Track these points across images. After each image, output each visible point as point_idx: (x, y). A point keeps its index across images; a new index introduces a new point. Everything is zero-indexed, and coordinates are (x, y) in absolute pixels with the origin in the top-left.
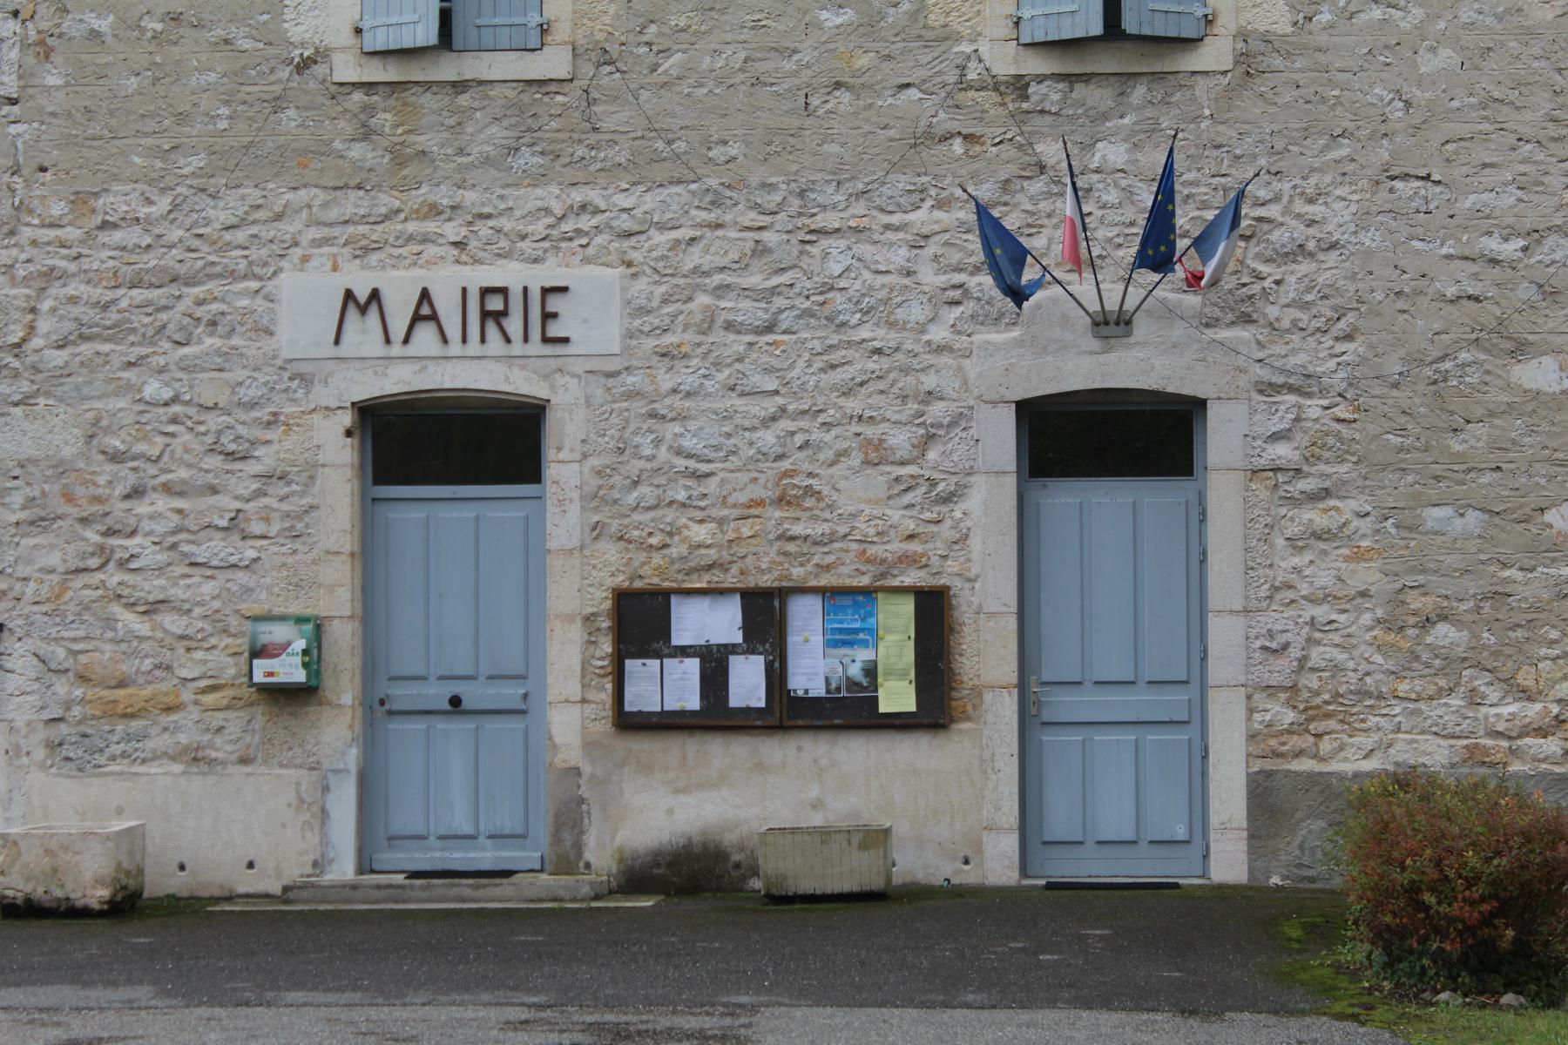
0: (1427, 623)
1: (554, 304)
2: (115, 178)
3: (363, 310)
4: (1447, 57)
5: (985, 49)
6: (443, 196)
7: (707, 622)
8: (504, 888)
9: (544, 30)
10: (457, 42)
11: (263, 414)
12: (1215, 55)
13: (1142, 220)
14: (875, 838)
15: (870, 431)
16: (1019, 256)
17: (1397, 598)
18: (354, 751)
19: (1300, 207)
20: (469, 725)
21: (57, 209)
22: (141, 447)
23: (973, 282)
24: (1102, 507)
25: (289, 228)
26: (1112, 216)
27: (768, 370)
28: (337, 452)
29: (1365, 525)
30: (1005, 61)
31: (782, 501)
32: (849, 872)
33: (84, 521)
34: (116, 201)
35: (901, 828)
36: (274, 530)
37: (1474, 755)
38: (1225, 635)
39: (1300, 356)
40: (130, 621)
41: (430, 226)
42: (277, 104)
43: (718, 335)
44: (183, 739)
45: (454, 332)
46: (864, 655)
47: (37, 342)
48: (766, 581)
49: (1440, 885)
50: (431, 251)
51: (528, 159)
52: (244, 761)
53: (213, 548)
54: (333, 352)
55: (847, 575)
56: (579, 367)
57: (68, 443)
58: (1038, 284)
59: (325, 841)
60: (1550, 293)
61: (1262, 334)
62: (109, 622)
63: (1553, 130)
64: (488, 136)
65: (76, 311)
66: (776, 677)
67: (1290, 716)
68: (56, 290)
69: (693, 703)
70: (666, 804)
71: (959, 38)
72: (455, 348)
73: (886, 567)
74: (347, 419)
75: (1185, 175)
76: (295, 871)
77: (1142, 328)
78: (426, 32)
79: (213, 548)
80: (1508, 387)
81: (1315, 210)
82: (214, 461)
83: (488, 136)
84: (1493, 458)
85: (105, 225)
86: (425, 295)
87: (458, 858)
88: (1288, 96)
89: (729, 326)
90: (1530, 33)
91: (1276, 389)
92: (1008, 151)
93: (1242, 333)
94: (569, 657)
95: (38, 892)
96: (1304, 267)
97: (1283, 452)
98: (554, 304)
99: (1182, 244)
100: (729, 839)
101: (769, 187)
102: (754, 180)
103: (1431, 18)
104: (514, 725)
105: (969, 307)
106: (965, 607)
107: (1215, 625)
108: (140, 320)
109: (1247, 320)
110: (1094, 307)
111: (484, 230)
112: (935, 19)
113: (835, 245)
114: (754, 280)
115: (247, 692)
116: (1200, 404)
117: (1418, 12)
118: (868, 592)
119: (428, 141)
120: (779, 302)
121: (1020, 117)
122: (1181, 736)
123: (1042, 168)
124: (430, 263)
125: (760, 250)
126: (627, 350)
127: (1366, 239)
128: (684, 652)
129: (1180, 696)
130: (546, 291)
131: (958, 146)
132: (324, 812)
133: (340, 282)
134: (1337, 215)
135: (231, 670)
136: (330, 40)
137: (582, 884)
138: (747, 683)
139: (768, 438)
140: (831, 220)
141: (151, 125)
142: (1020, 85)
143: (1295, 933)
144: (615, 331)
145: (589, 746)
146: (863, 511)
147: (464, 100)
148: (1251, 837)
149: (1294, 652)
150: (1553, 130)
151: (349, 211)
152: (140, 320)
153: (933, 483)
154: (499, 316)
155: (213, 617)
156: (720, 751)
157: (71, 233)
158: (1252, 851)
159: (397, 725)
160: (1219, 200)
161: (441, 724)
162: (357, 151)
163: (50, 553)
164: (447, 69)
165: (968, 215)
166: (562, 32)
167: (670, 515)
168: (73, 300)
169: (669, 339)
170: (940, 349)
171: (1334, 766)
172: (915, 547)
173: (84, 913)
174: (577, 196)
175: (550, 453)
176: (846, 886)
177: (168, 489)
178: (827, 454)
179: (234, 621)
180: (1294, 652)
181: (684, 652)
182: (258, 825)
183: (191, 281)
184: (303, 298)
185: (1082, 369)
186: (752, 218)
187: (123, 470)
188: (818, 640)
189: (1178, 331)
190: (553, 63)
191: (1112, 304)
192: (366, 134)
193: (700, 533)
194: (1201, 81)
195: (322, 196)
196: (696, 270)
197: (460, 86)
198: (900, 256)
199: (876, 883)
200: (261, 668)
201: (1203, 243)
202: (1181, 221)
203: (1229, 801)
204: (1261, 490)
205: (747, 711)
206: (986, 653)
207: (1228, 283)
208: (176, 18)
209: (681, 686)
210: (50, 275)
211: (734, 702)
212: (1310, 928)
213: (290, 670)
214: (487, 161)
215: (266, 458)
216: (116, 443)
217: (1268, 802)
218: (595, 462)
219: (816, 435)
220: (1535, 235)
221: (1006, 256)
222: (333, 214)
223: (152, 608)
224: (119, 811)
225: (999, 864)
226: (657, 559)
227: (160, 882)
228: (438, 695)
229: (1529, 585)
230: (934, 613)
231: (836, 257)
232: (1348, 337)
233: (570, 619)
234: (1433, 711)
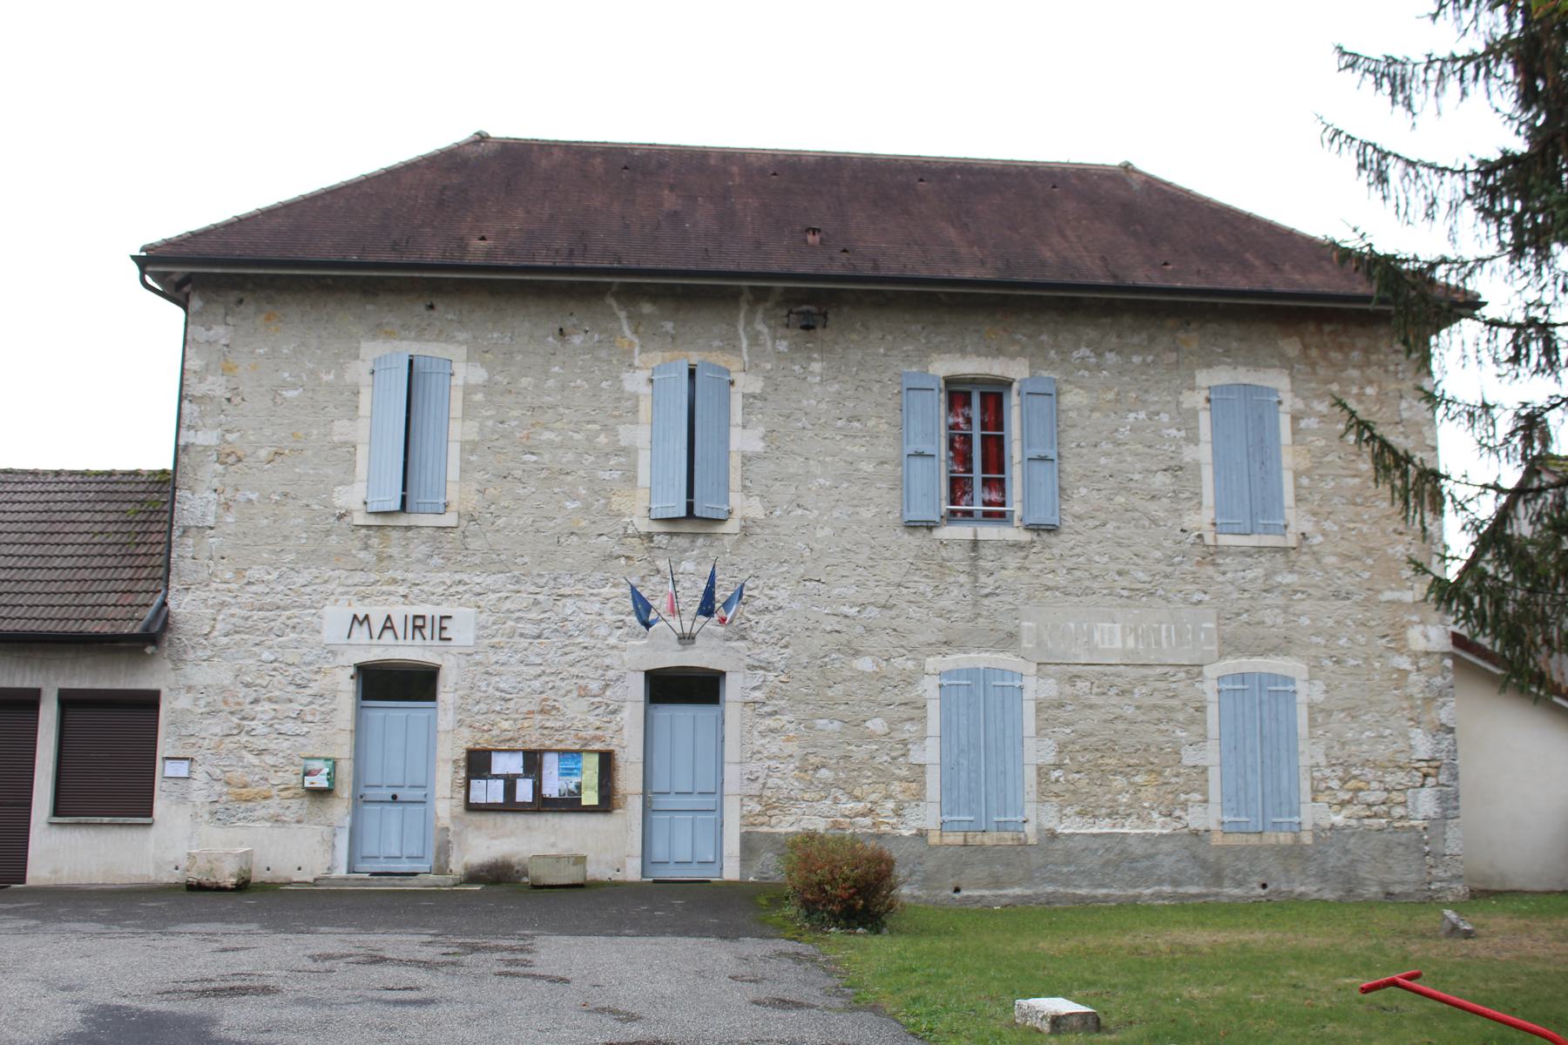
1: (446, 623)
3: (361, 623)
4: (828, 531)
5: (635, 520)
6: (399, 575)
8: (414, 880)
9: (446, 506)
10: (408, 508)
11: (314, 668)
12: (732, 526)
13: (700, 595)
14: (580, 860)
16: (648, 608)
17: (804, 758)
18: (348, 818)
20: (400, 807)
21: (228, 575)
22: (259, 681)
23: (627, 619)
24: (682, 717)
25: (330, 587)
26: (688, 593)
27: (538, 655)
28: (346, 687)
29: (791, 727)
30: (644, 526)
31: (542, 711)
32: (567, 875)
34: (254, 573)
37: (836, 825)
38: (732, 773)
39: (767, 654)
40: (250, 758)
41: (392, 588)
42: (328, 533)
43: (517, 639)
44: (271, 811)
45: (400, 634)
46: (576, 780)
47: (215, 633)
48: (534, 746)
50: (392, 598)
51: (437, 560)
52: (299, 822)
53: (289, 727)
54: (346, 641)
56: (455, 651)
57: (226, 678)
58: (656, 621)
59: (333, 859)
60: (869, 630)
61: (750, 644)
62: (241, 758)
64: (419, 550)
65: (233, 620)
66: (537, 789)
67: (759, 808)
68: (225, 611)
69: (500, 800)
72: (401, 641)
73: (587, 741)
74: (352, 671)
75: (719, 576)
77: (699, 640)
78: (396, 505)
79: (289, 727)
80: (851, 669)
81: (773, 593)
82: (292, 688)
83: (419, 550)
85: (249, 583)
86: (389, 618)
88: (762, 544)
89: (521, 635)
90: (861, 523)
91: (756, 668)
95: (204, 879)
96: (768, 617)
97: (758, 695)
98: (446, 623)
99: (717, 605)
100: (514, 860)
101: (541, 576)
102: (535, 572)
104: (420, 808)
106: (621, 759)
107: (727, 768)
108: (262, 625)
109: (743, 638)
111: (416, 590)
112: (614, 507)
113: (568, 601)
114: (533, 615)
115: (301, 791)
116: (723, 674)
117: (816, 512)
118: (578, 752)
119: (394, 551)
120: (544, 625)
122: (712, 816)
123: (658, 571)
125: (536, 603)
126: (476, 644)
127: (793, 605)
128: (497, 777)
129: (711, 799)
130: (442, 618)
131: (623, 561)
132: (334, 846)
134: (782, 595)
135: (294, 780)
137: (449, 879)
138: (524, 791)
139: (537, 684)
140: (567, 591)
141: (272, 540)
145: (454, 818)
146: (577, 718)
147: (410, 534)
149: (761, 781)
151: (357, 580)
152: (262, 625)
153: (608, 705)
154: (420, 628)
157: (233, 586)
158: (742, 866)
160: (732, 587)
161: (387, 807)
162: (362, 554)
163: (216, 727)
164: (403, 520)
165: (627, 590)
166: (454, 506)
167: (493, 716)
168: (233, 615)
169: (495, 640)
170: (613, 647)
171: (777, 830)
172: (599, 733)
173: (224, 889)
174: (457, 577)
176: (567, 881)
177: (270, 700)
178: (562, 692)
179: (297, 760)
180: (761, 781)
181: (497, 777)
182: (303, 850)
183: (285, 609)
184: (335, 618)
187: (250, 691)
188: (556, 773)
189: (715, 642)
190: (449, 519)
191: (687, 631)
192: (366, 547)
193: (506, 725)
195: (346, 573)
196: (508, 610)
197: (408, 528)
199: (580, 880)
200: (308, 781)
201: (727, 605)
203: (732, 845)
205: (524, 803)
206: (629, 780)
207: (736, 622)
209: (494, 792)
210: (223, 604)
211: (519, 799)
212: (770, 900)
213: (321, 782)
214: (419, 561)
215: (315, 688)
216: (248, 679)
217: (749, 845)
218: (460, 693)
219: (558, 683)
221: (642, 608)
222: (350, 582)
223: (260, 753)
224: (241, 843)
225: (632, 872)
226: (486, 736)
227: (259, 876)
228: (386, 794)
229: (860, 753)
230: (607, 761)
231: (569, 606)
232: (786, 647)
233: (446, 761)
234: (819, 806)
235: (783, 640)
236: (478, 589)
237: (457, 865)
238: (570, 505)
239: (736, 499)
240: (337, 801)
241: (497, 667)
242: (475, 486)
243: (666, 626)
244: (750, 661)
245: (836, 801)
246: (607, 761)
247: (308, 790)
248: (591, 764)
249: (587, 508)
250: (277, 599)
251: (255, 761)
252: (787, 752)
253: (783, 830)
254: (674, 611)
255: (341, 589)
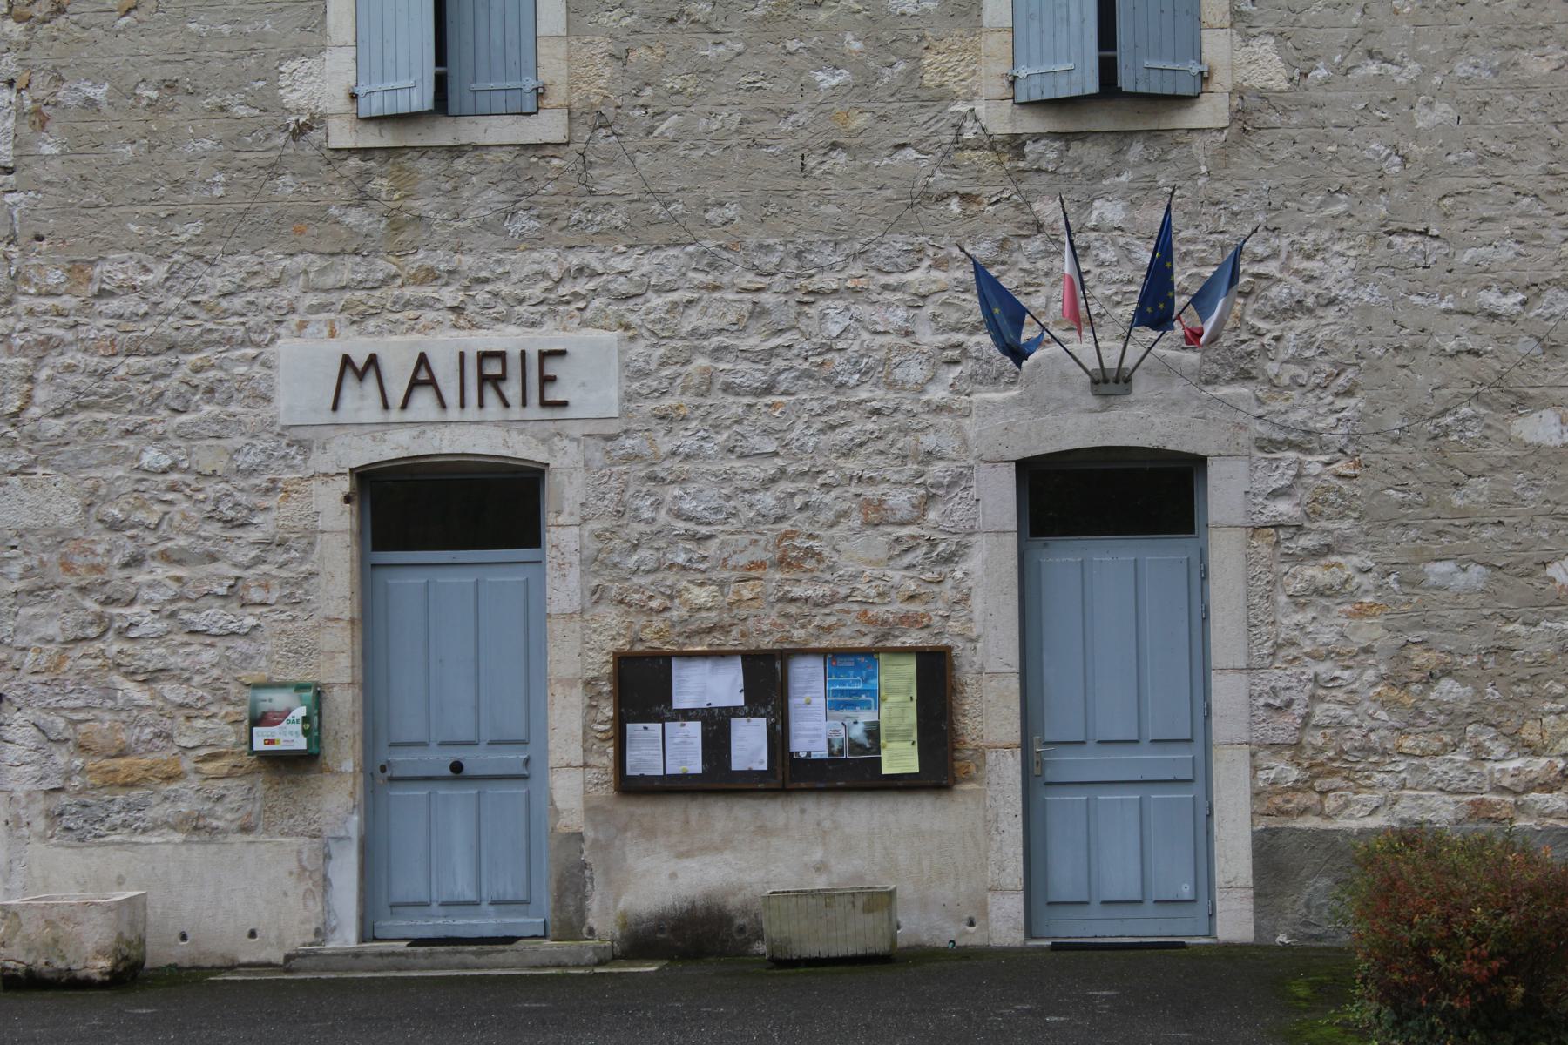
0: (1431, 679)
1: (552, 367)
2: (112, 246)
3: (361, 376)
4: (1443, 111)
5: (980, 109)
7: (710, 685)
8: (508, 955)
9: (539, 94)
10: (453, 106)
11: (261, 480)
12: (1211, 112)
13: (1140, 277)
14: (880, 901)
15: (870, 492)
16: (1018, 315)
17: (1400, 654)
18: (356, 818)
19: (1298, 263)
20: (471, 790)
21: (54, 277)
22: (139, 516)
24: (1105, 566)
26: (1110, 274)
27: (767, 432)
28: (334, 517)
29: (1367, 581)
30: (1000, 120)
31: (782, 562)
32: (854, 935)
33: (83, 590)
34: (114, 269)
35: (906, 891)
36: (273, 597)
38: (1228, 692)
40: (130, 690)
41: (428, 291)
42: (273, 170)
43: (717, 398)
44: (184, 807)
45: (452, 396)
46: (866, 716)
47: (34, 411)
48: (767, 643)
49: (1449, 943)
50: (429, 316)
51: (524, 223)
52: (246, 829)
53: (212, 616)
54: (329, 417)
55: (846, 637)
56: (577, 430)
57: (66, 512)
58: (1037, 343)
59: (327, 909)
60: (1550, 347)
62: (109, 691)
63: (1550, 184)
64: (484, 201)
65: (73, 380)
66: (779, 739)
67: (1294, 774)
69: (696, 766)
70: (670, 869)
71: (954, 98)
72: (454, 413)
73: (887, 628)
74: (345, 485)
75: (1183, 231)
76: (297, 938)
78: (421, 98)
79: (212, 616)
80: (1509, 441)
81: (1313, 266)
82: (213, 529)
83: (484, 201)
84: (1495, 513)
85: (102, 294)
86: (423, 360)
87: (461, 924)
88: (1284, 152)
89: (728, 388)
90: (1526, 87)
91: (1277, 445)
92: (1006, 211)
93: (1242, 390)
94: (569, 720)
96: (1303, 323)
97: (1284, 508)
98: (552, 367)
99: (1180, 301)
100: (733, 903)
101: (765, 248)
102: (751, 242)
103: (1426, 72)
104: (517, 790)
105: (967, 367)
106: (966, 672)
107: (1218, 683)
108: (138, 388)
109: (1246, 376)
110: (1093, 365)
111: (481, 293)
112: (930, 79)
113: (833, 306)
114: (752, 341)
115: (247, 760)
116: (1200, 462)
117: (1413, 67)
118: (870, 653)
119: (424, 206)
120: (778, 364)
121: (1016, 176)
122: (1185, 795)
123: (1039, 227)
124: (428, 328)
125: (758, 311)
126: (625, 413)
127: (1364, 294)
128: (686, 715)
129: (1183, 755)
130: (544, 355)
131: (955, 206)
132: (326, 880)
133: (338, 347)
134: (1336, 271)
136: (325, 106)
137: (587, 949)
138: (749, 745)
140: (829, 281)
141: (148, 193)
142: (1016, 144)
143: (1303, 992)
144: (614, 394)
145: (592, 810)
146: (864, 570)
147: (460, 164)
148: (1257, 895)
149: (1298, 709)
150: (1550, 184)
152: (138, 388)
153: (933, 544)
154: (497, 381)
155: (213, 685)
156: (723, 815)
158: (1259, 910)
159: (399, 792)
160: (1216, 256)
161: (443, 791)
162: (354, 217)
163: (49, 623)
164: (443, 134)
165: (966, 274)
166: (557, 95)
167: (670, 578)
168: (71, 369)
169: (668, 402)
170: (940, 409)
171: (1339, 823)
172: (916, 607)
174: (574, 259)
175: (549, 517)
176: (851, 949)
177: (166, 557)
178: (826, 516)
179: (233, 689)
180: (1298, 709)
181: (686, 715)
183: (188, 349)
184: (301, 364)
185: (1082, 427)
186: (748, 279)
187: (122, 539)
188: (820, 702)
189: (1178, 388)
190: (548, 126)
191: (1111, 362)
192: (363, 199)
193: (701, 596)
194: (1198, 141)
195: (319, 262)
197: (456, 151)
198: (898, 316)
199: (882, 946)
200: (261, 736)
201: (1202, 300)
202: (1179, 279)
204: (1262, 546)
205: (750, 774)
206: (990, 714)
207: (1227, 340)
208: (171, 86)
209: (682, 749)
210: (47, 344)
211: (737, 764)
214: (484, 225)
215: (265, 526)
217: (1274, 860)
218: (594, 525)
219: (816, 497)
220: (1534, 290)
221: (1004, 316)
222: (330, 280)
223: (151, 677)
224: (120, 882)
225: (1004, 925)
226: (658, 622)
227: (162, 952)
228: (438, 761)
230: (936, 673)
231: (834, 318)
232: (1348, 393)
233: (569, 683)
234: (1439, 767)
235: (1338, 373)
236: (622, 285)
237: (605, 915)
238: (827, 80)
239: (1217, 46)
240: (329, 780)
241: (676, 464)
242: (604, 45)
243: (1065, 355)
244: (1261, 429)
245: (1479, 754)
246: (936, 673)
247: (265, 757)
248: (898, 685)
249: (864, 86)
250: (168, 327)
251: (141, 695)
252: (1360, 639)
253: (1354, 825)
254: (1079, 319)
255: (311, 299)
